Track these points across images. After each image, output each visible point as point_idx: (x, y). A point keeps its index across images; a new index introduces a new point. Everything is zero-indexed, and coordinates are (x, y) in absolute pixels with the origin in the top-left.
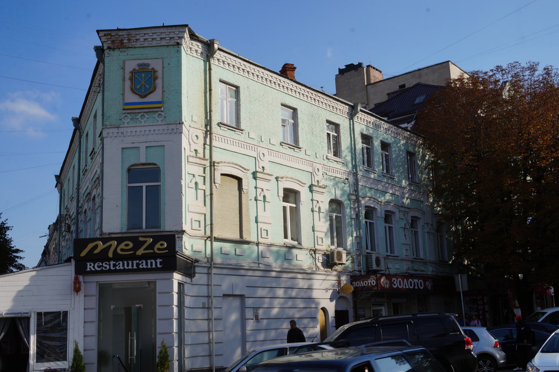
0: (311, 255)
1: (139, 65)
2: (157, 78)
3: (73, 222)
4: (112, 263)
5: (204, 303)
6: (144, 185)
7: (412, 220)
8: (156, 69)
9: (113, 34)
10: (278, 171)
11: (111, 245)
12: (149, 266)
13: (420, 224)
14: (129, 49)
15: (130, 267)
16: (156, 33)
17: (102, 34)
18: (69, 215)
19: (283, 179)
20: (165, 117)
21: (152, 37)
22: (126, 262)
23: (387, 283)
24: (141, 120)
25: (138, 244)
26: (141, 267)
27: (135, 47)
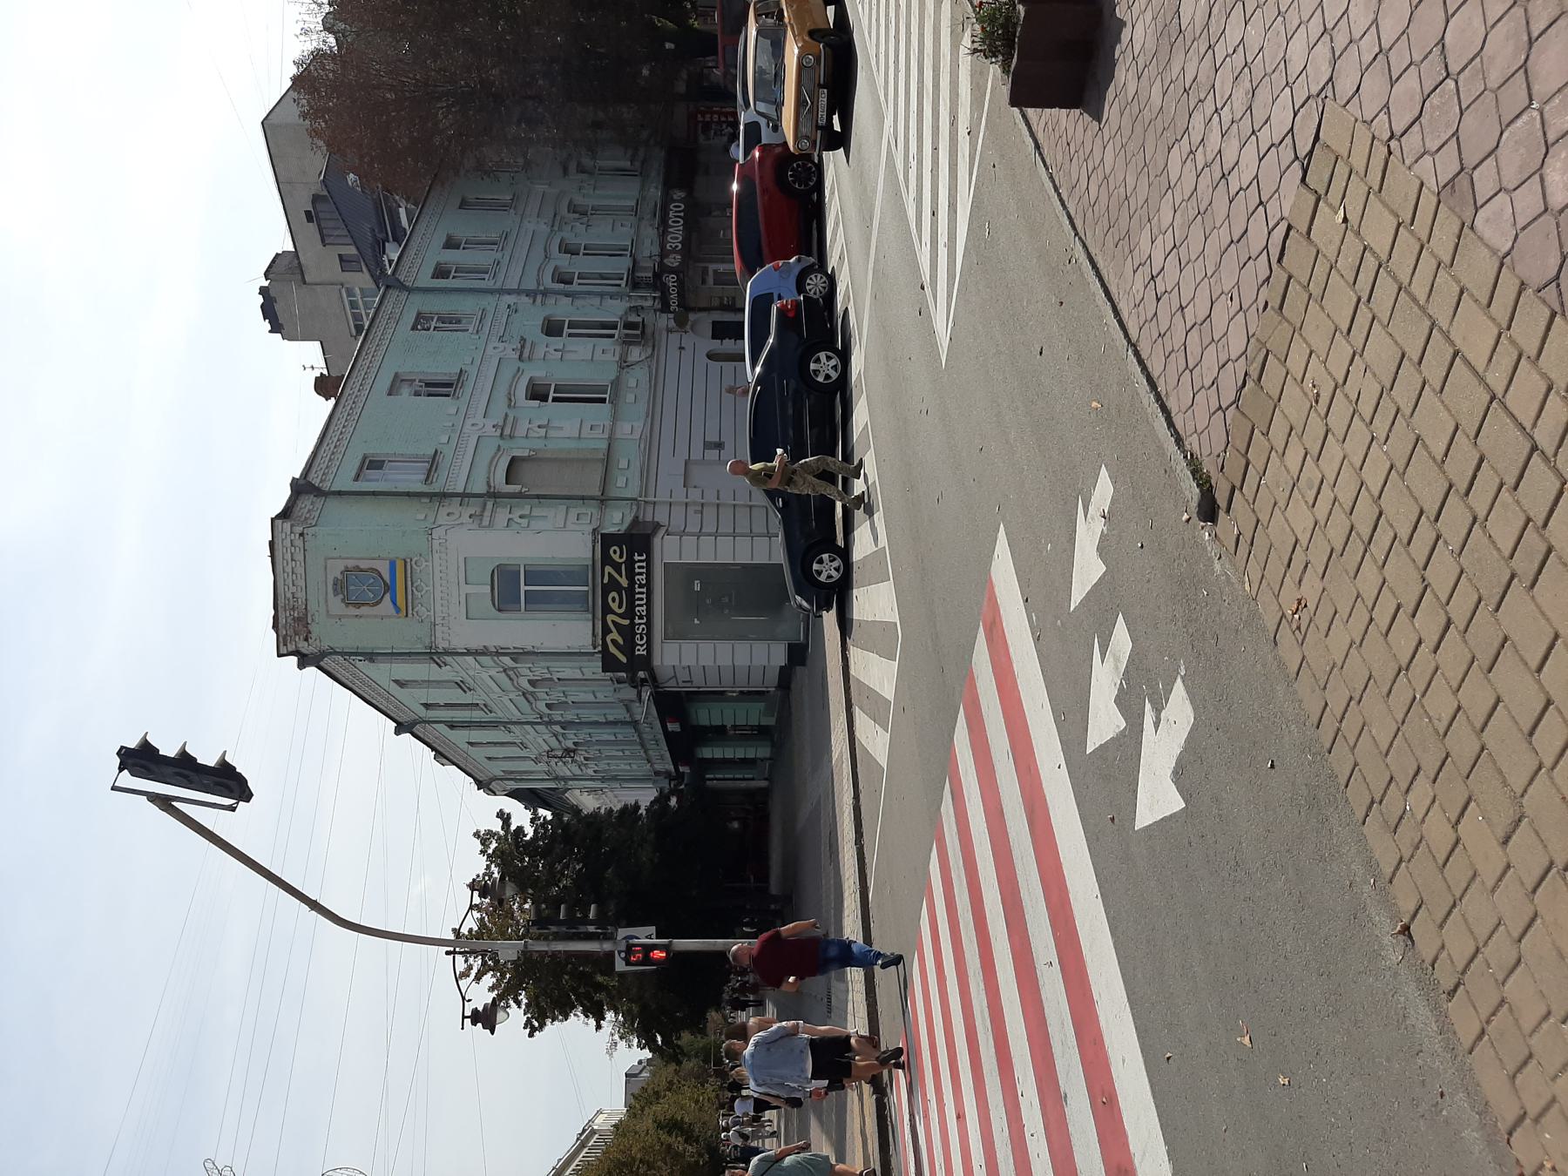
0: (628, 366)
1: (336, 593)
2: (358, 567)
3: (561, 738)
4: (637, 621)
5: (696, 512)
6: (523, 588)
7: (574, 212)
8: (343, 569)
9: (284, 633)
10: (500, 406)
11: (613, 621)
12: (644, 570)
13: (579, 200)
14: (309, 608)
15: (644, 596)
17: (284, 651)
18: (548, 751)
19: (513, 399)
21: (291, 574)
22: (637, 602)
23: (674, 258)
24: (424, 592)
25: (613, 585)
26: (644, 582)
27: (306, 600)
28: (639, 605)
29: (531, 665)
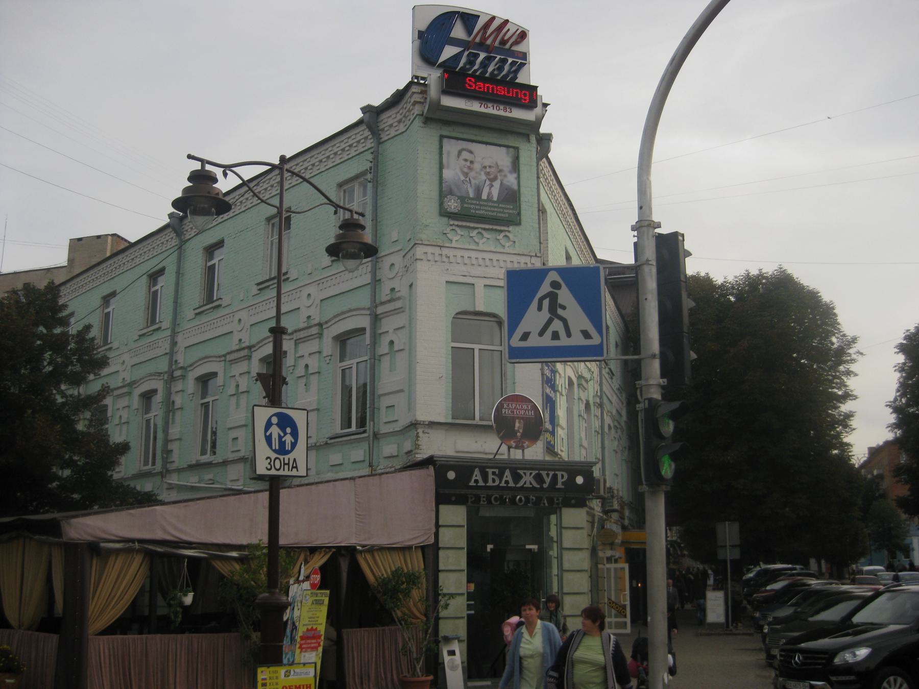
6: (476, 347)
20: (515, 242)
29: (325, 354)
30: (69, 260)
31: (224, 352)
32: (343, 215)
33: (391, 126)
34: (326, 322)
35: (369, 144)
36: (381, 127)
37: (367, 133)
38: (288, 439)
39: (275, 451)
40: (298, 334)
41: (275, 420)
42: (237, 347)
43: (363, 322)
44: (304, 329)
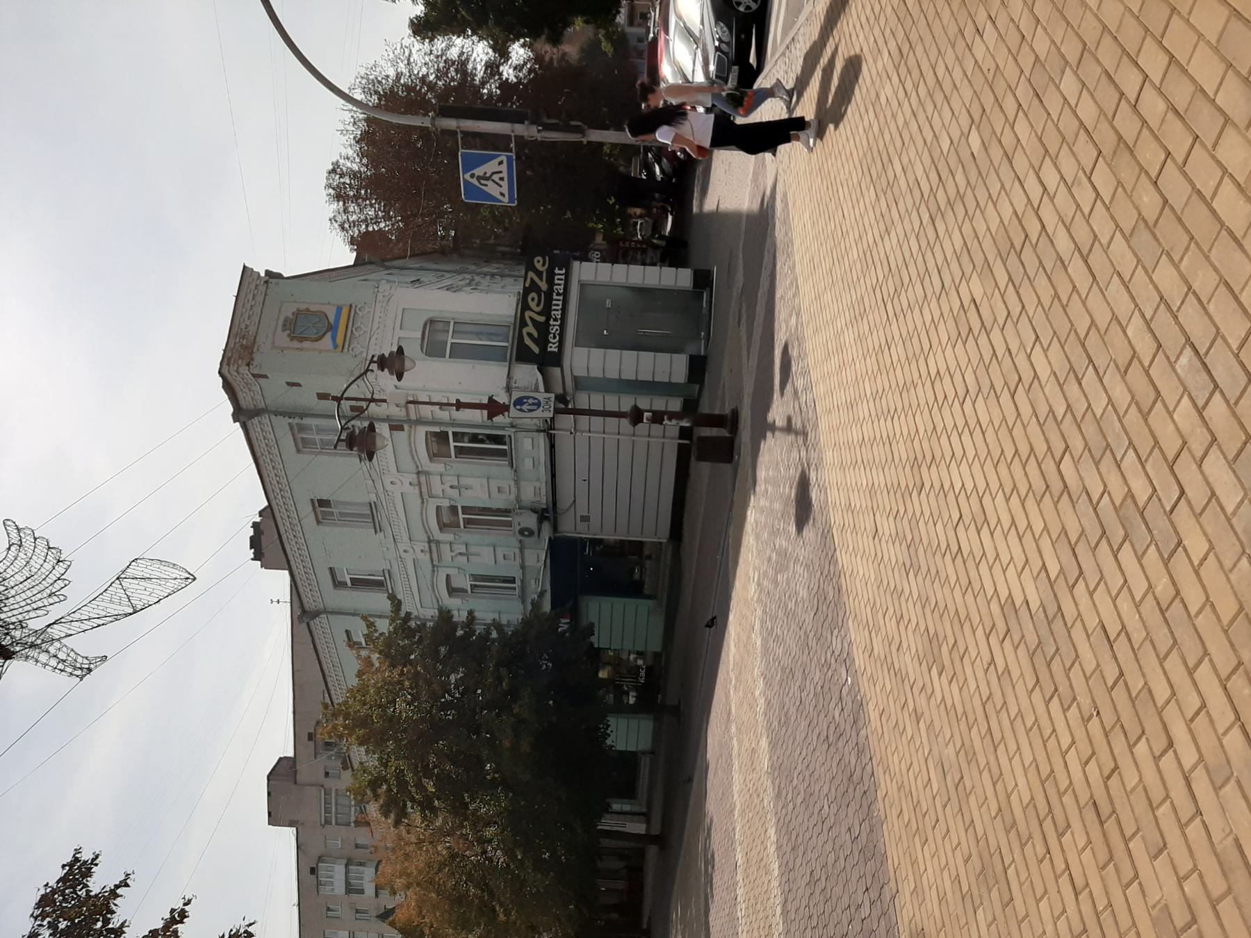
1: (284, 330)
4: (552, 322)
6: (450, 341)
8: (295, 310)
11: (530, 318)
14: (257, 340)
15: (560, 303)
16: (244, 304)
22: (554, 307)
25: (534, 287)
26: (561, 291)
27: (256, 333)
28: (555, 310)
30: (290, 826)
31: (430, 566)
32: (374, 366)
33: (253, 398)
34: (417, 467)
35: (265, 419)
36: (252, 406)
37: (255, 421)
38: (531, 401)
39: (538, 408)
40: (423, 493)
41: (518, 407)
42: (428, 554)
43: (421, 431)
44: (420, 488)
